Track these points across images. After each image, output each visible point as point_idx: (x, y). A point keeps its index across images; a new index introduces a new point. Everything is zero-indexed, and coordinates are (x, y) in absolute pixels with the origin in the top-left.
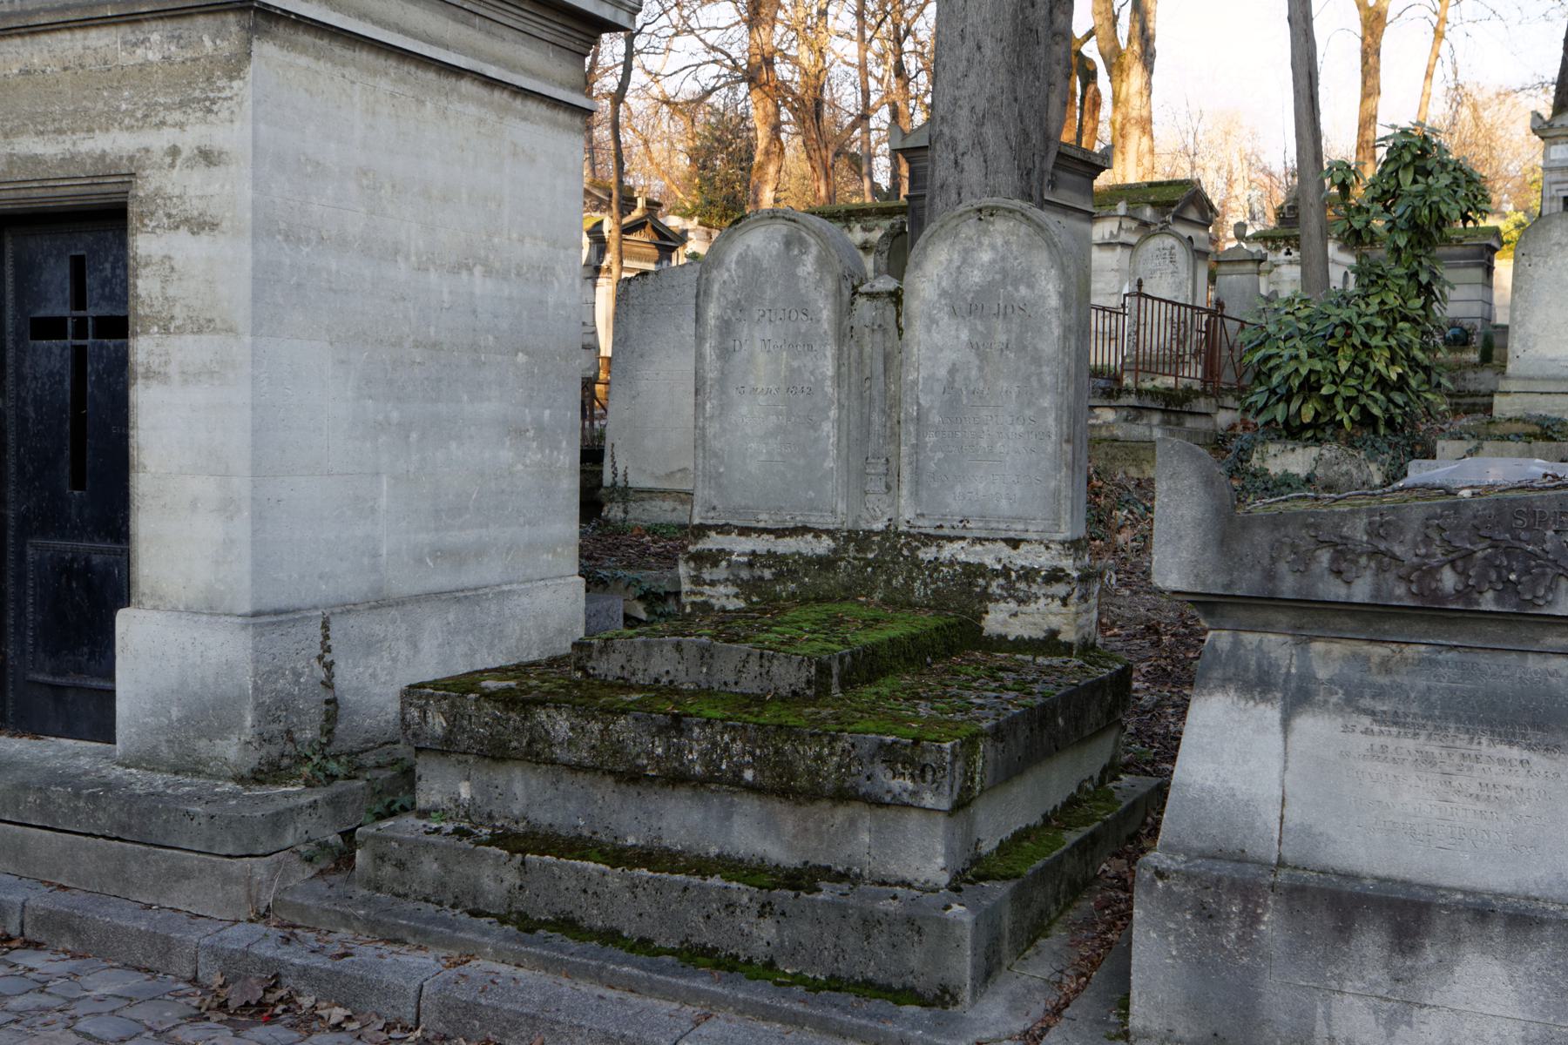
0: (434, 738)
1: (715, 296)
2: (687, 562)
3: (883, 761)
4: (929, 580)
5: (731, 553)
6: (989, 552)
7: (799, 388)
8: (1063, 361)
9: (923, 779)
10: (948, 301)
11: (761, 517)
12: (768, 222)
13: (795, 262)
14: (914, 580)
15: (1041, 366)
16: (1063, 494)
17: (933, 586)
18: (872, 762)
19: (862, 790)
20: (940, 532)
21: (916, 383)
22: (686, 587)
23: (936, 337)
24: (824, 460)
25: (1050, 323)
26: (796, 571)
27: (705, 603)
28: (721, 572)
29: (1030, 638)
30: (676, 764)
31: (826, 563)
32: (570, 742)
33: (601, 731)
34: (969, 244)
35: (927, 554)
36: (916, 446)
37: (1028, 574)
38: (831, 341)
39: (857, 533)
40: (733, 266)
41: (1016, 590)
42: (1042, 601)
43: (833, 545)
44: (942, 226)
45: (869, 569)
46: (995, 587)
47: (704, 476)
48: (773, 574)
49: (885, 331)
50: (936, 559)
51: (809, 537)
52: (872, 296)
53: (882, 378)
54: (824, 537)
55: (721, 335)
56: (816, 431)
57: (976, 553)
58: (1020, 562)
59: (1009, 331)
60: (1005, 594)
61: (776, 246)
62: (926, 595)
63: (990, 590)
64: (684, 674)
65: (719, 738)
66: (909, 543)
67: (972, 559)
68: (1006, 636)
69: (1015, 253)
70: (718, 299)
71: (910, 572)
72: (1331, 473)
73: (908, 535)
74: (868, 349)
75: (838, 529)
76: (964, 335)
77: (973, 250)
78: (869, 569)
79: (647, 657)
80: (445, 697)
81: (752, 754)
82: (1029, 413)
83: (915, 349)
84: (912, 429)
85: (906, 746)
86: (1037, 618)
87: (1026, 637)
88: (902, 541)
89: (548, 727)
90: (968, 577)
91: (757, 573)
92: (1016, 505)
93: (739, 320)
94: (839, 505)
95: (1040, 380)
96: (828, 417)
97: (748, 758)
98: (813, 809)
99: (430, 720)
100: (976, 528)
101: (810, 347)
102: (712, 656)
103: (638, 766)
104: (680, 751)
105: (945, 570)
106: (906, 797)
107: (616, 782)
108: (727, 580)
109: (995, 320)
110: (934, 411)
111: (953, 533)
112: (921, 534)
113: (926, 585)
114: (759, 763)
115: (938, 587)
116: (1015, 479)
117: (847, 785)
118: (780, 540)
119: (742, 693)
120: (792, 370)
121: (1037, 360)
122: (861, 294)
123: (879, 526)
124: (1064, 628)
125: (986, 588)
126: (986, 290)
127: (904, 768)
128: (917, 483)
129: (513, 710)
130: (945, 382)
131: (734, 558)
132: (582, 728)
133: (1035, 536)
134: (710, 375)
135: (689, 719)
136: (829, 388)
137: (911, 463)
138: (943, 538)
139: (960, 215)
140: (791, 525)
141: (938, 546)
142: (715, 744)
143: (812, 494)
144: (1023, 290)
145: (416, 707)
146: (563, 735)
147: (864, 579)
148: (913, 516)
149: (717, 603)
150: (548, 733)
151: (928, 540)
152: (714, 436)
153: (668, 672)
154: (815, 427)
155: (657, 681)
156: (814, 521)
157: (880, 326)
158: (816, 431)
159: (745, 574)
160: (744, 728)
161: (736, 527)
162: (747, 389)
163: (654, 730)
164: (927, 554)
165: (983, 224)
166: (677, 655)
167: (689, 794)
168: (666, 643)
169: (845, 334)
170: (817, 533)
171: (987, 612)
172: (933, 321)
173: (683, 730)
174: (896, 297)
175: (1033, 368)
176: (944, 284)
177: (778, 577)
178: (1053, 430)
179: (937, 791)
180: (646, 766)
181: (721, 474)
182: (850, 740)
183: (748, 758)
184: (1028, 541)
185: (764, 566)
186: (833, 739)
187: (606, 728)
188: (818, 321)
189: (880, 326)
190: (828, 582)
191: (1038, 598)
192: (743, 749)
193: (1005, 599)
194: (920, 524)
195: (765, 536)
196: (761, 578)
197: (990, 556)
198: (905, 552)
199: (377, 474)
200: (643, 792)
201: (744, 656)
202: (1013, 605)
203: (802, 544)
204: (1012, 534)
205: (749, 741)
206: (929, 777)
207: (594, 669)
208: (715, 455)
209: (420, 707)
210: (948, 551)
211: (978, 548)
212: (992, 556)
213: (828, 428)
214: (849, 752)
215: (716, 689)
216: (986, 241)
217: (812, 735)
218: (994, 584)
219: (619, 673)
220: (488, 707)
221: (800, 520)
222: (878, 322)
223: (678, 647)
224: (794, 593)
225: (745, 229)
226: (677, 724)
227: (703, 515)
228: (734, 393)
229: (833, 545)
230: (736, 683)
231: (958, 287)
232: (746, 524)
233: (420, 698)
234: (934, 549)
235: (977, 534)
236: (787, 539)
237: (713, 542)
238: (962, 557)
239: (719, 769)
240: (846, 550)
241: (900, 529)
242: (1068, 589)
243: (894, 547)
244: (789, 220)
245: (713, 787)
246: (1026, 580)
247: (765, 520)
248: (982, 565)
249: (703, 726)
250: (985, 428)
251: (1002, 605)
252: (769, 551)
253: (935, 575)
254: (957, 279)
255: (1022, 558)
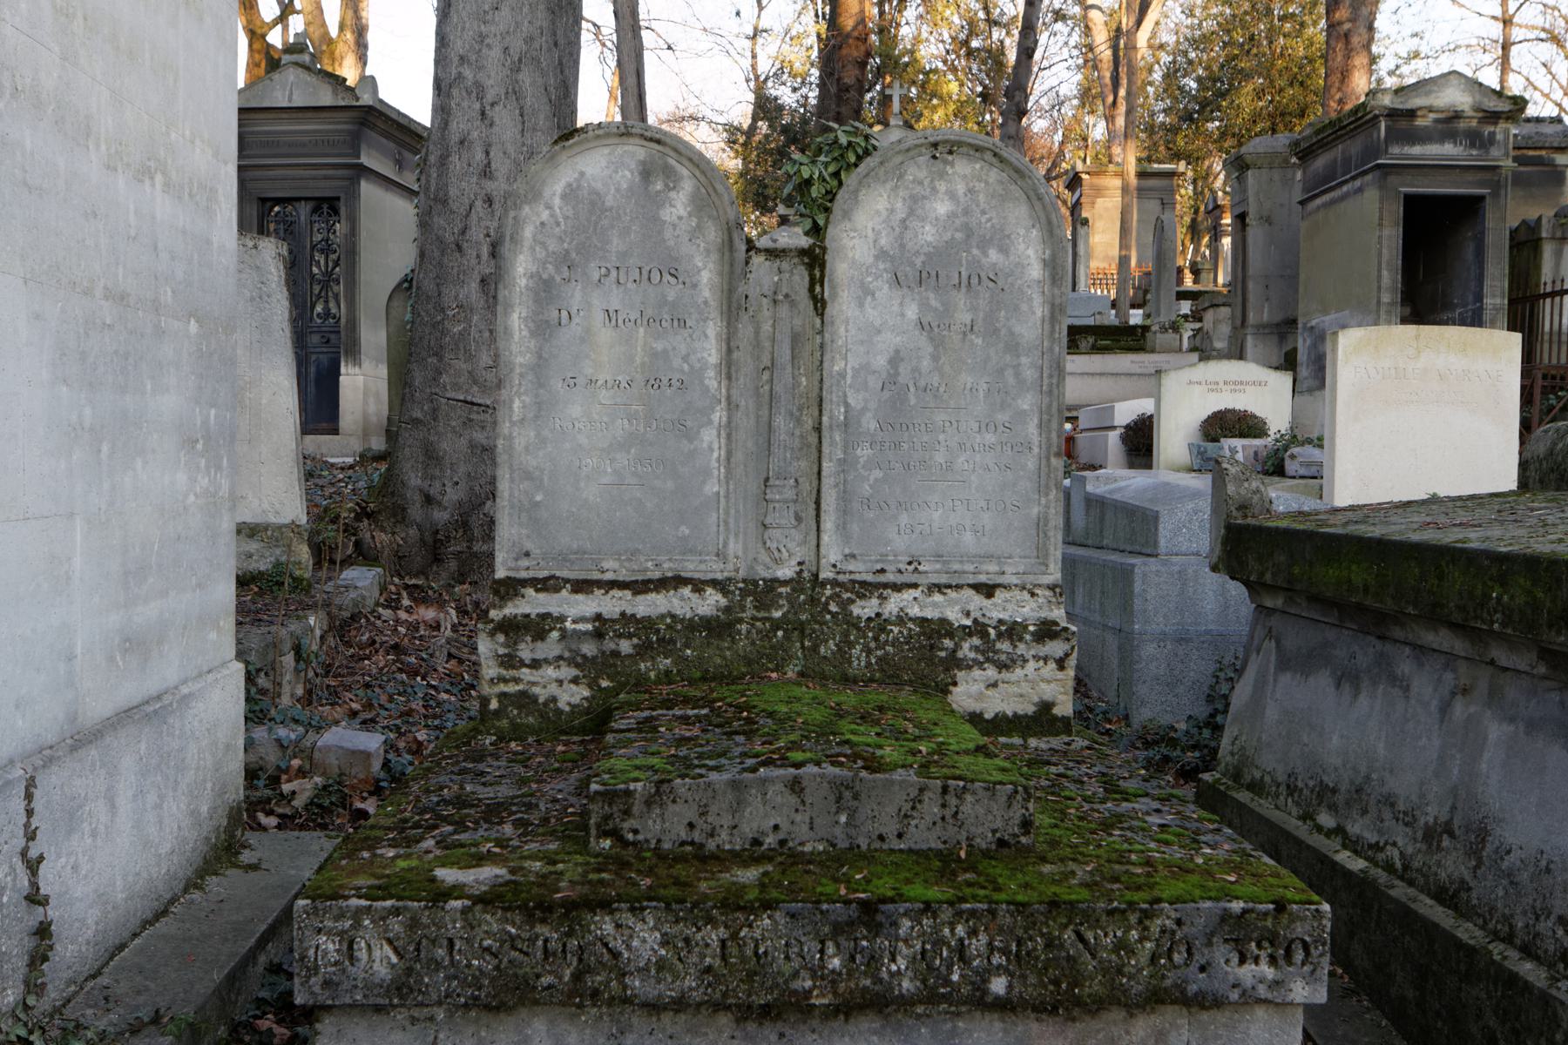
0: (369, 986)
1: (527, 244)
2: (492, 634)
3: (1226, 941)
4: (873, 645)
5: (562, 619)
6: (952, 603)
7: (665, 381)
8: (1051, 349)
9: (1289, 962)
10: (888, 265)
11: (606, 565)
12: (616, 140)
13: (658, 201)
14: (851, 645)
15: (1018, 356)
16: (1052, 524)
17: (879, 653)
18: (1209, 944)
19: (1192, 988)
20: (882, 578)
21: (842, 375)
22: (490, 670)
23: (872, 314)
24: (704, 482)
25: (1030, 299)
26: (672, 641)
27: (523, 694)
28: (551, 646)
29: (1015, 714)
30: (868, 982)
31: (717, 627)
32: (661, 965)
33: (723, 943)
34: (918, 189)
35: (864, 609)
36: (842, 462)
37: (1012, 631)
38: (715, 314)
39: (755, 583)
40: (557, 201)
41: (996, 652)
42: (1031, 665)
43: (723, 601)
44: (882, 163)
45: (780, 633)
46: (966, 650)
47: (512, 507)
48: (635, 646)
49: (793, 304)
50: (878, 615)
51: (686, 591)
52: (773, 254)
53: (789, 369)
54: (709, 591)
55: (537, 301)
56: (691, 441)
57: (935, 605)
58: (997, 615)
59: (974, 309)
60: (981, 658)
61: (627, 176)
62: (869, 664)
63: (960, 654)
64: (805, 828)
65: (947, 931)
66: (838, 595)
67: (929, 614)
68: (981, 714)
69: (982, 205)
70: (532, 249)
71: (846, 634)
72: (1243, 492)
73: (835, 583)
74: (767, 327)
75: (729, 579)
76: (912, 312)
77: (924, 197)
78: (780, 633)
79: (738, 806)
80: (396, 912)
81: (1005, 952)
82: (1002, 417)
83: (842, 330)
84: (838, 438)
85: (1266, 914)
86: (1025, 688)
87: (1010, 713)
88: (828, 592)
89: (618, 944)
90: (930, 638)
91: (609, 645)
92: (985, 540)
93: (567, 281)
94: (731, 545)
95: (1017, 375)
96: (710, 422)
97: (997, 959)
98: (1095, 1024)
99: (363, 955)
100: (932, 571)
101: (683, 323)
102: (856, 797)
103: (795, 992)
104: (873, 960)
105: (896, 630)
106: (1262, 991)
107: (738, 1021)
108: (560, 658)
109: (954, 293)
110: (869, 415)
111: (900, 579)
112: (854, 582)
113: (869, 652)
114: (1020, 961)
115: (887, 654)
116: (983, 504)
117: (1168, 982)
118: (640, 598)
119: (910, 851)
120: (655, 355)
121: (1013, 347)
122: (759, 251)
123: (786, 572)
124: (1061, 697)
125: (954, 651)
126: (941, 254)
127: (1259, 946)
128: (844, 511)
129: (543, 921)
130: (884, 375)
131: (568, 624)
132: (687, 940)
133: (1014, 580)
134: (519, 360)
135: (890, 906)
136: (712, 381)
137: (836, 485)
138: (885, 586)
139: (908, 150)
140: (657, 575)
141: (881, 597)
142: (940, 942)
143: (685, 530)
144: (994, 255)
145: (329, 933)
146: (646, 955)
147: (772, 647)
148: (840, 557)
149: (542, 694)
150: (615, 955)
151: (865, 589)
152: (527, 449)
153: (776, 827)
154: (690, 435)
155: (756, 842)
156: (691, 568)
157: (787, 296)
158: (691, 441)
159: (589, 649)
160: (993, 913)
161: (567, 581)
162: (581, 381)
163: (826, 929)
164: (864, 609)
165: (939, 165)
166: (793, 800)
167: (876, 1025)
168: (772, 781)
169: (733, 306)
170: (698, 586)
171: (955, 684)
172: (867, 292)
173: (881, 925)
174: (814, 260)
175: (1008, 358)
176: (883, 242)
177: (644, 650)
178: (1035, 439)
179: (1311, 978)
180: (810, 991)
181: (537, 504)
182: (1173, 915)
183: (997, 959)
184: (1006, 587)
185: (620, 636)
186: (1147, 915)
187: (734, 936)
188: (695, 286)
189: (787, 296)
190: (718, 656)
191: (1025, 661)
192: (990, 944)
193: (980, 665)
194: (851, 568)
195: (616, 593)
196: (616, 654)
197: (953, 609)
198: (833, 608)
199: (72, 514)
200: (788, 1031)
201: (914, 793)
202: (991, 672)
203: (676, 601)
204: (983, 578)
205: (1001, 930)
206: (1299, 956)
207: (636, 832)
208: (528, 476)
209: (341, 933)
210: (894, 604)
211: (937, 597)
212: (957, 608)
213: (709, 436)
214: (1173, 933)
215: (864, 847)
216: (942, 187)
217: (1111, 913)
218: (966, 645)
219: (684, 835)
220: (491, 921)
221: (669, 569)
222: (785, 291)
223: (795, 786)
224: (668, 673)
225: (577, 149)
226: (871, 914)
227: (513, 565)
228: (558, 385)
229: (723, 601)
230: (900, 836)
231: (902, 246)
232: (582, 576)
233: (340, 916)
234: (875, 601)
235: (935, 579)
236: (652, 596)
237: (531, 604)
238: (915, 611)
239: (947, 982)
240: (743, 609)
241: (822, 576)
242: (1066, 647)
243: (813, 601)
244: (651, 140)
245: (920, 1010)
246: (1011, 638)
247: (613, 568)
248: (944, 621)
249: (916, 917)
250: (941, 437)
251: (977, 673)
252: (623, 614)
253: (883, 637)
254: (901, 236)
255: (998, 610)
